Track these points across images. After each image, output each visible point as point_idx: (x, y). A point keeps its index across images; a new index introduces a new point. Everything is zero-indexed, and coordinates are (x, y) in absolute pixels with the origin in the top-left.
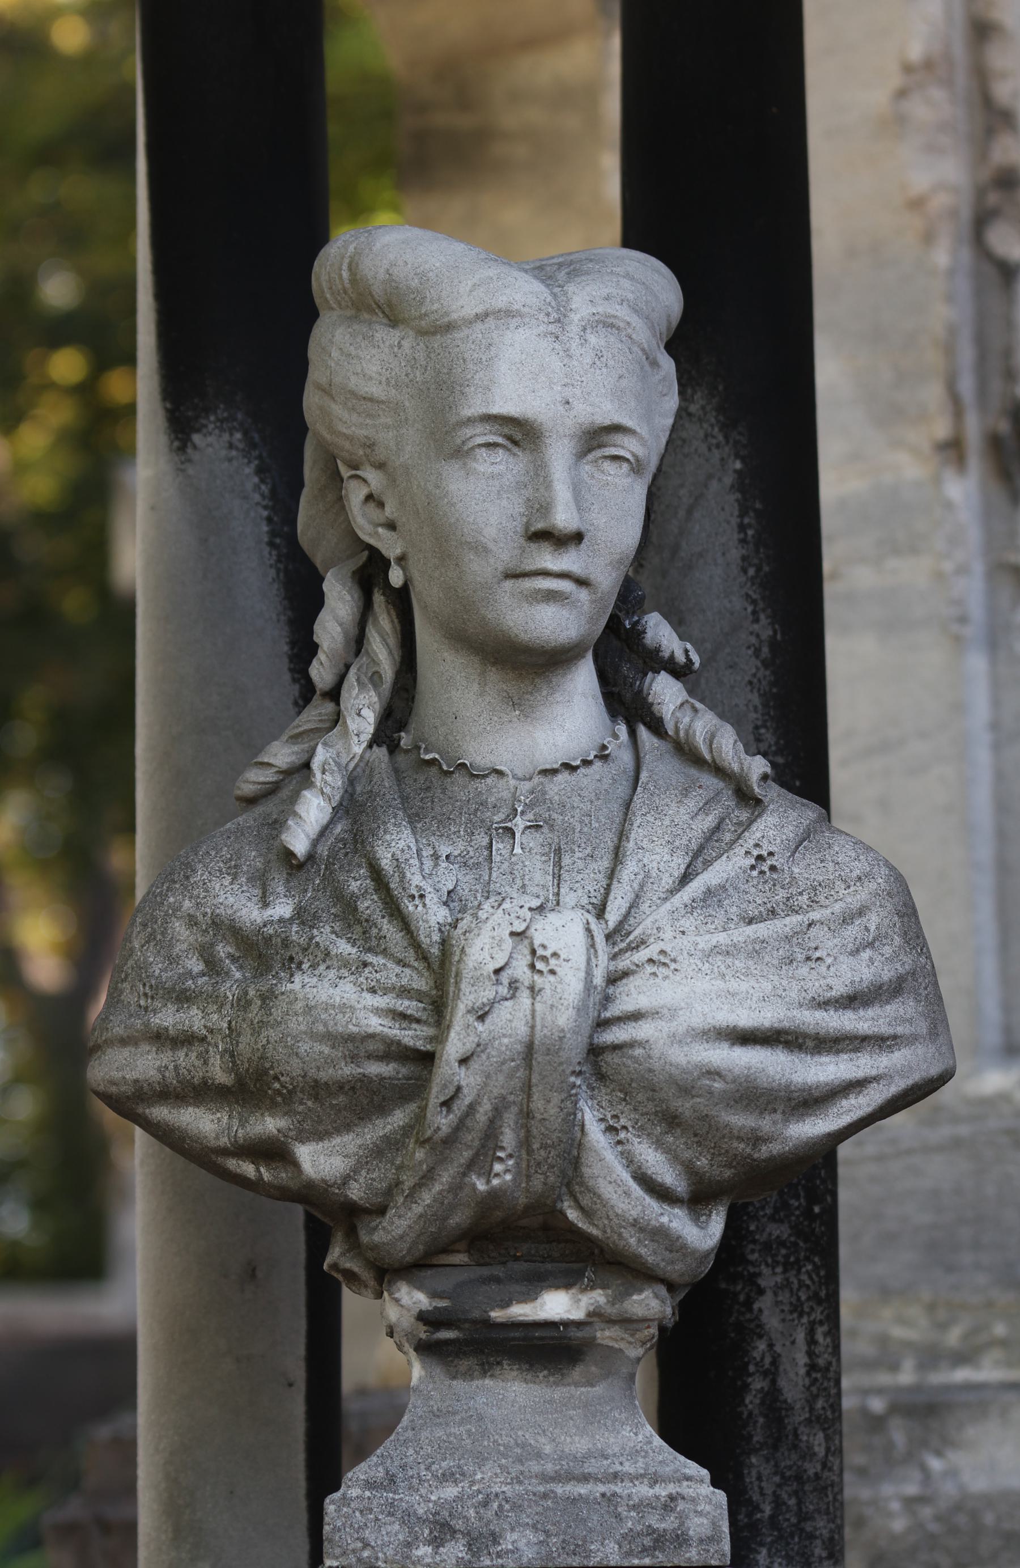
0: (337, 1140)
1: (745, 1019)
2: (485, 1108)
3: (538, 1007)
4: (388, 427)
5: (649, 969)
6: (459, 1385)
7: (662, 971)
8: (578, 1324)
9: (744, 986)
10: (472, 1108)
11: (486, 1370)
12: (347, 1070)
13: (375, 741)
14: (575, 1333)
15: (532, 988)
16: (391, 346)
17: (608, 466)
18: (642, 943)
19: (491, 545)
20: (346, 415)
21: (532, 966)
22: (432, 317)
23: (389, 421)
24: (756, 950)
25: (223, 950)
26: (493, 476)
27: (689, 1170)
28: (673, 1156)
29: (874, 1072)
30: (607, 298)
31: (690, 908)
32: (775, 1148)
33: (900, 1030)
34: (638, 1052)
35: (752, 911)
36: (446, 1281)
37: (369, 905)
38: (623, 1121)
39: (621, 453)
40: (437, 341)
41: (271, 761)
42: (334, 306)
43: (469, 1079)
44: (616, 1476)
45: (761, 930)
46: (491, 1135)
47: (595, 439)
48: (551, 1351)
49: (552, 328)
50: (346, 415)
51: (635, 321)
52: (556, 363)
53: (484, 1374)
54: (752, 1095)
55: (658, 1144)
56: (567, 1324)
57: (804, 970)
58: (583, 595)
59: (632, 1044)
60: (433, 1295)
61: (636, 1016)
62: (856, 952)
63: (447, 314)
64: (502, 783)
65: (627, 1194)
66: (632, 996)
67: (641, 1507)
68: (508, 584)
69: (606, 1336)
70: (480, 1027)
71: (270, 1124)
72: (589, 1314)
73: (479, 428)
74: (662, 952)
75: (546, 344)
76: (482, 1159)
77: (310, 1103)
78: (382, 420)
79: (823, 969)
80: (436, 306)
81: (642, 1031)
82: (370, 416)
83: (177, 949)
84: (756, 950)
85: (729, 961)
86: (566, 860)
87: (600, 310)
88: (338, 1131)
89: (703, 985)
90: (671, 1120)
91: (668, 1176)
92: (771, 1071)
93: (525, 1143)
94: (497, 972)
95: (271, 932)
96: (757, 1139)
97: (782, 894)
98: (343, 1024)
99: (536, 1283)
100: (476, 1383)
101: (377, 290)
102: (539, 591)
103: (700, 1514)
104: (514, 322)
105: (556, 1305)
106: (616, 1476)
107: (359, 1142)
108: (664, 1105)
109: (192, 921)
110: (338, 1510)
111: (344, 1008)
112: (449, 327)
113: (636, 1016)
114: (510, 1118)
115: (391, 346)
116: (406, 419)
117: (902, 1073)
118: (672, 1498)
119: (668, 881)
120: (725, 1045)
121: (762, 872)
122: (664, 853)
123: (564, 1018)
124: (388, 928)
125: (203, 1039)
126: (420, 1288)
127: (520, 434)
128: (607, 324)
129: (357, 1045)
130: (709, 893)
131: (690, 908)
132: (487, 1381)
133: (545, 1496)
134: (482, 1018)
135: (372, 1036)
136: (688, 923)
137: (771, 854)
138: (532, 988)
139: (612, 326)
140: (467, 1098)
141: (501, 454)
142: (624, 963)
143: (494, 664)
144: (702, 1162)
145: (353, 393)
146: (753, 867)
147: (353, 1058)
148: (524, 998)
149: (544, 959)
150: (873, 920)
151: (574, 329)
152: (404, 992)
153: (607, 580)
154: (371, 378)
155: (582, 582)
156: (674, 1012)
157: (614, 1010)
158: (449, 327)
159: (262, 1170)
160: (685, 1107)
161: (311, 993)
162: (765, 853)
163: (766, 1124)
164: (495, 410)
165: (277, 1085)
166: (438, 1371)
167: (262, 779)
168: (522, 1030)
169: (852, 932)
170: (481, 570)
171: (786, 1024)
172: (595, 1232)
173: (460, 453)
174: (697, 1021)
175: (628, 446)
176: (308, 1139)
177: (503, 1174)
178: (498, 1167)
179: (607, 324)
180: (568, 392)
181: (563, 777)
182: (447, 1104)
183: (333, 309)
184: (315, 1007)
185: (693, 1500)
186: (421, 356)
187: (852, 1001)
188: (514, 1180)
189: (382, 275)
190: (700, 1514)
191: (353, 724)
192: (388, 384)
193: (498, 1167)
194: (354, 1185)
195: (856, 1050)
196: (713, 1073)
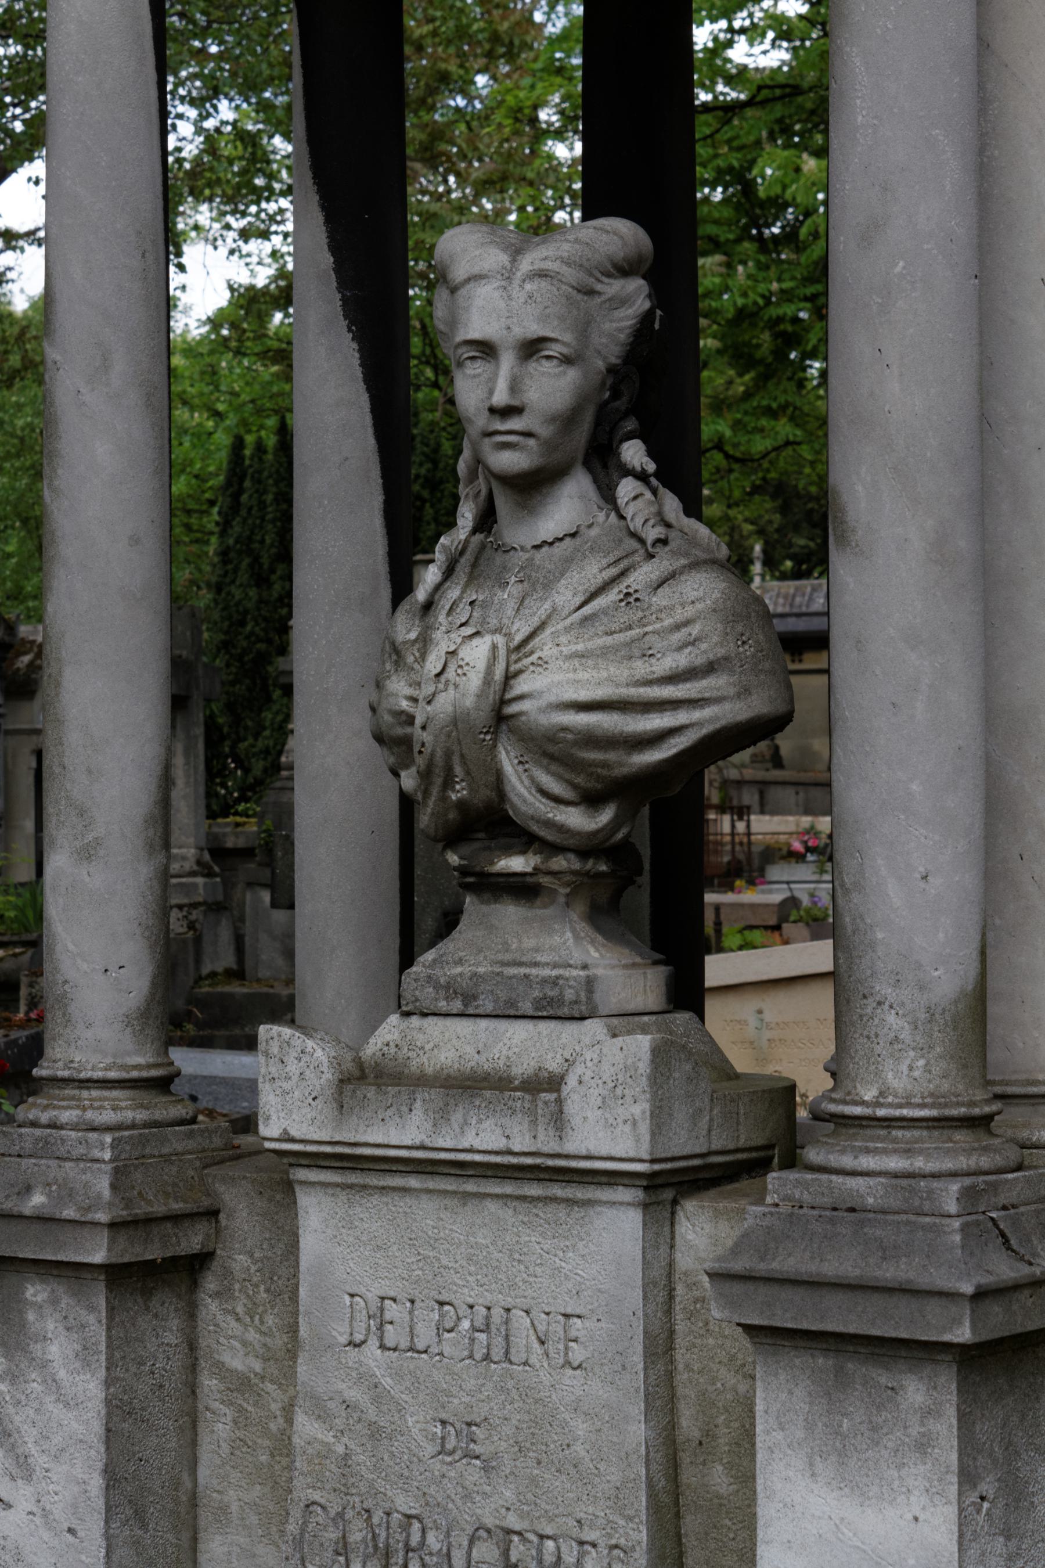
1: (584, 695)
2: (439, 753)
5: (532, 668)
6: (485, 908)
7: (540, 669)
8: (531, 874)
9: (587, 676)
10: (433, 754)
11: (496, 899)
13: (474, 531)
14: (529, 879)
17: (544, 362)
18: (532, 653)
24: (604, 653)
26: (475, 376)
27: (575, 787)
28: (559, 777)
29: (688, 722)
30: (545, 259)
31: (567, 630)
32: (625, 770)
33: (707, 695)
34: (524, 718)
35: (614, 627)
36: (467, 849)
38: (526, 758)
39: (551, 353)
43: (426, 737)
44: (536, 964)
45: (609, 640)
46: (449, 770)
47: (531, 349)
48: (523, 889)
49: (503, 283)
51: (565, 270)
52: (502, 304)
53: (496, 902)
54: (591, 739)
55: (549, 772)
56: (524, 875)
57: (639, 663)
58: (532, 442)
59: (521, 714)
60: (461, 858)
61: (521, 697)
62: (680, 649)
65: (525, 801)
66: (521, 686)
67: (544, 981)
68: (487, 440)
69: (545, 880)
70: (429, 708)
72: (535, 869)
73: (464, 349)
74: (540, 658)
75: (497, 294)
76: (448, 782)
79: (653, 661)
81: (524, 706)
84: (604, 653)
85: (584, 661)
86: (527, 602)
87: (536, 267)
89: (558, 677)
90: (552, 757)
91: (556, 787)
92: (606, 725)
93: (468, 773)
94: (438, 675)
96: (605, 765)
97: (640, 614)
99: (509, 851)
102: (498, 443)
103: (570, 987)
104: (483, 282)
105: (517, 863)
106: (536, 964)
108: (550, 749)
113: (521, 697)
114: (456, 760)
117: (710, 720)
118: (557, 977)
119: (566, 612)
120: (572, 712)
121: (629, 603)
122: (569, 594)
123: (469, 702)
127: (486, 349)
128: (542, 274)
130: (586, 619)
131: (567, 630)
133: (498, 974)
134: (429, 703)
135: (403, 712)
136: (563, 639)
137: (636, 591)
139: (546, 276)
140: (427, 750)
141: (479, 363)
142: (513, 668)
144: (579, 780)
146: (621, 601)
148: (451, 691)
149: (460, 667)
150: (695, 630)
151: (517, 282)
153: (545, 432)
155: (528, 434)
156: (541, 693)
157: (508, 696)
160: (551, 749)
162: (631, 590)
163: (611, 756)
164: (469, 337)
168: (450, 709)
169: (677, 637)
171: (615, 698)
174: (553, 699)
175: (554, 350)
177: (459, 792)
178: (458, 787)
179: (542, 274)
180: (509, 322)
181: (545, 549)
182: (420, 752)
185: (567, 979)
187: (672, 678)
188: (469, 793)
190: (570, 987)
191: (460, 522)
193: (458, 787)
195: (675, 709)
196: (565, 729)
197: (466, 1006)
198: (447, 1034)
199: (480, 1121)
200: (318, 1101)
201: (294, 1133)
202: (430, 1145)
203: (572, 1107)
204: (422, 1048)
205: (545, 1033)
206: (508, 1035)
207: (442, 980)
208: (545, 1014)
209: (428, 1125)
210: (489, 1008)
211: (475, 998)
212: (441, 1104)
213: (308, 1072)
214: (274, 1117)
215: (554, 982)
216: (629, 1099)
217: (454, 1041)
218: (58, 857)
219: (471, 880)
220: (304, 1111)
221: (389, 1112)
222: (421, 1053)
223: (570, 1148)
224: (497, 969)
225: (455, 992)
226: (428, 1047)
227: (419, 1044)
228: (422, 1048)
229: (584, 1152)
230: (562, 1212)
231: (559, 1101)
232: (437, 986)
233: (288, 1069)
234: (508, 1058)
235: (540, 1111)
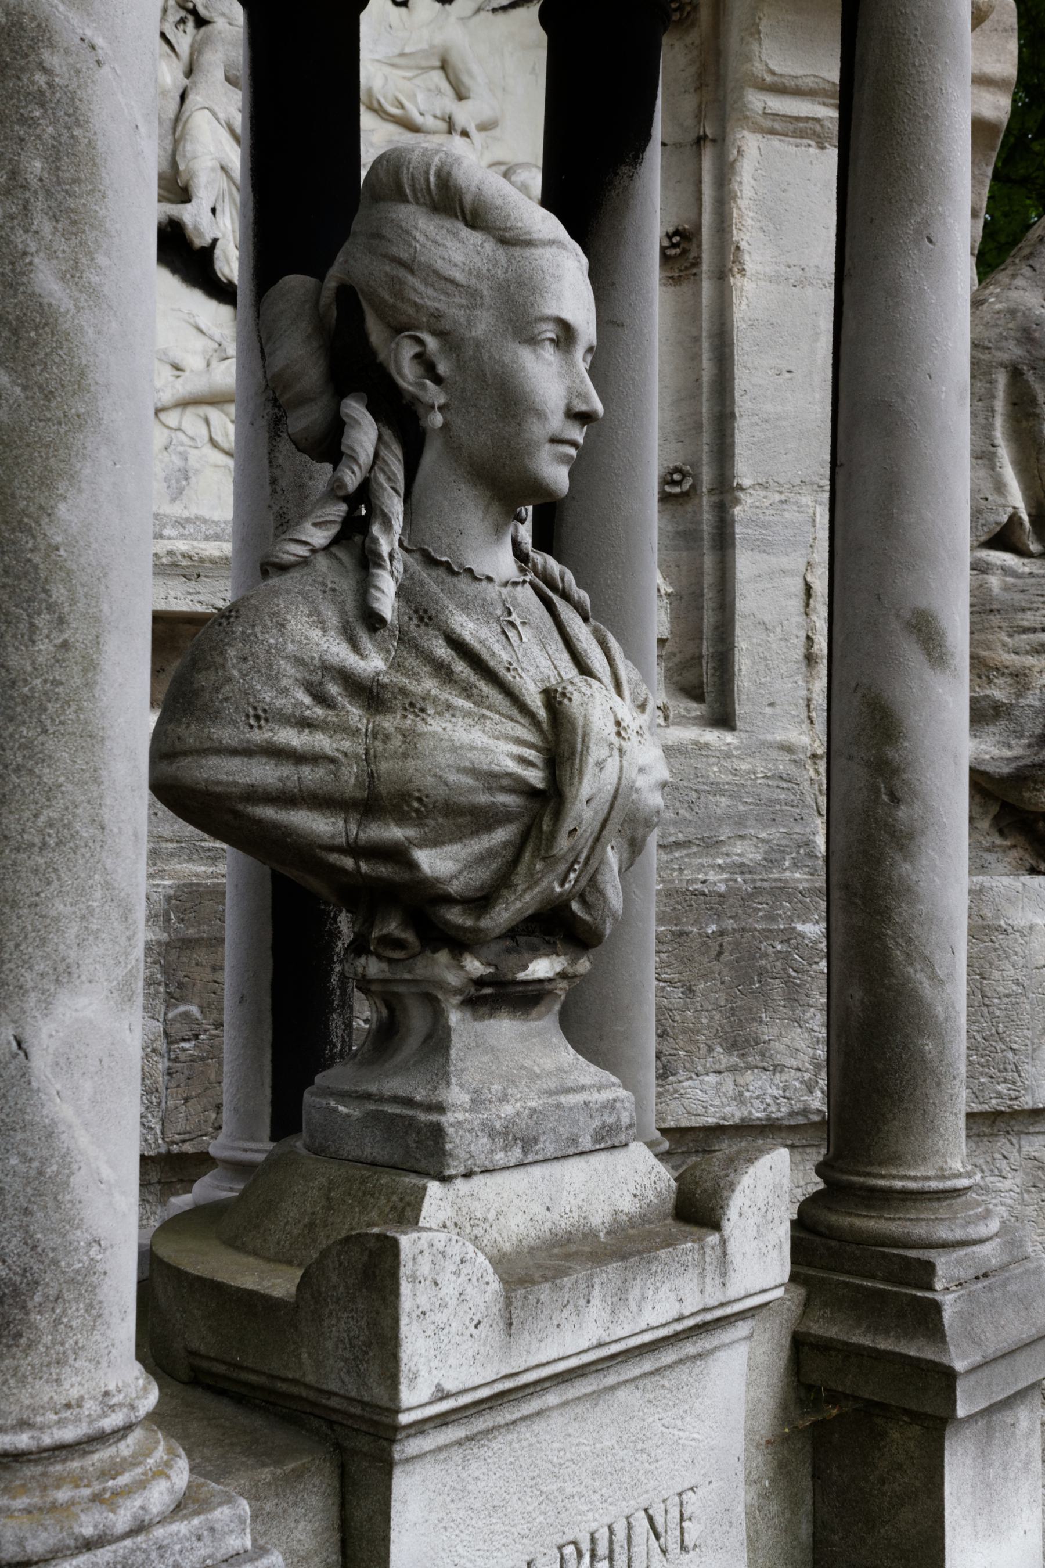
0: (447, 848)
3: (625, 763)
4: (462, 306)
6: (479, 1026)
8: (550, 980)
12: (483, 798)
14: (548, 986)
15: (620, 750)
16: (474, 245)
19: (549, 415)
20: (421, 287)
21: (619, 734)
22: (516, 232)
23: (464, 301)
25: (333, 689)
37: (460, 667)
40: (517, 251)
41: (309, 540)
42: (410, 197)
50: (421, 287)
53: (491, 1016)
63: (529, 233)
64: (490, 586)
68: (547, 447)
71: (396, 833)
77: (440, 820)
78: (457, 300)
80: (520, 225)
82: (448, 295)
83: (285, 682)
88: (451, 841)
95: (386, 680)
98: (483, 762)
100: (487, 1022)
101: (468, 199)
107: (469, 850)
109: (298, 661)
110: (457, 1132)
111: (486, 751)
112: (529, 243)
115: (474, 245)
116: (482, 305)
124: (485, 688)
125: (333, 760)
126: (478, 959)
129: (492, 779)
132: (492, 1021)
138: (620, 750)
143: (500, 500)
145: (436, 273)
147: (490, 789)
152: (519, 741)
154: (456, 265)
158: (529, 243)
159: (361, 864)
161: (456, 736)
165: (416, 805)
166: (468, 1015)
167: (301, 553)
170: (538, 431)
172: (587, 918)
173: (533, 341)
176: (426, 846)
183: (408, 202)
184: (461, 747)
186: (503, 261)
189: (473, 189)
192: (470, 274)
194: (455, 882)
197: (525, 1153)
198: (505, 1195)
199: (656, 1291)
200: (481, 1327)
201: (450, 1386)
202: (607, 1340)
203: (732, 1247)
204: (485, 1220)
205: (600, 1168)
206: (567, 1179)
207: (498, 1125)
208: (602, 1146)
209: (606, 1315)
210: (550, 1150)
211: (536, 1140)
212: (619, 1283)
213: (469, 1289)
214: (424, 1373)
215: (611, 1106)
216: (777, 1221)
217: (516, 1201)
218: (82, 1001)
219: (488, 991)
220: (464, 1347)
221: (566, 1313)
222: (487, 1226)
223: (732, 1293)
224: (552, 1101)
225: (515, 1139)
226: (491, 1216)
227: (479, 1216)
228: (485, 1220)
229: (743, 1293)
230: (682, 1374)
231: (724, 1242)
232: (492, 1134)
233: (444, 1291)
234: (580, 1208)
235: (708, 1259)
